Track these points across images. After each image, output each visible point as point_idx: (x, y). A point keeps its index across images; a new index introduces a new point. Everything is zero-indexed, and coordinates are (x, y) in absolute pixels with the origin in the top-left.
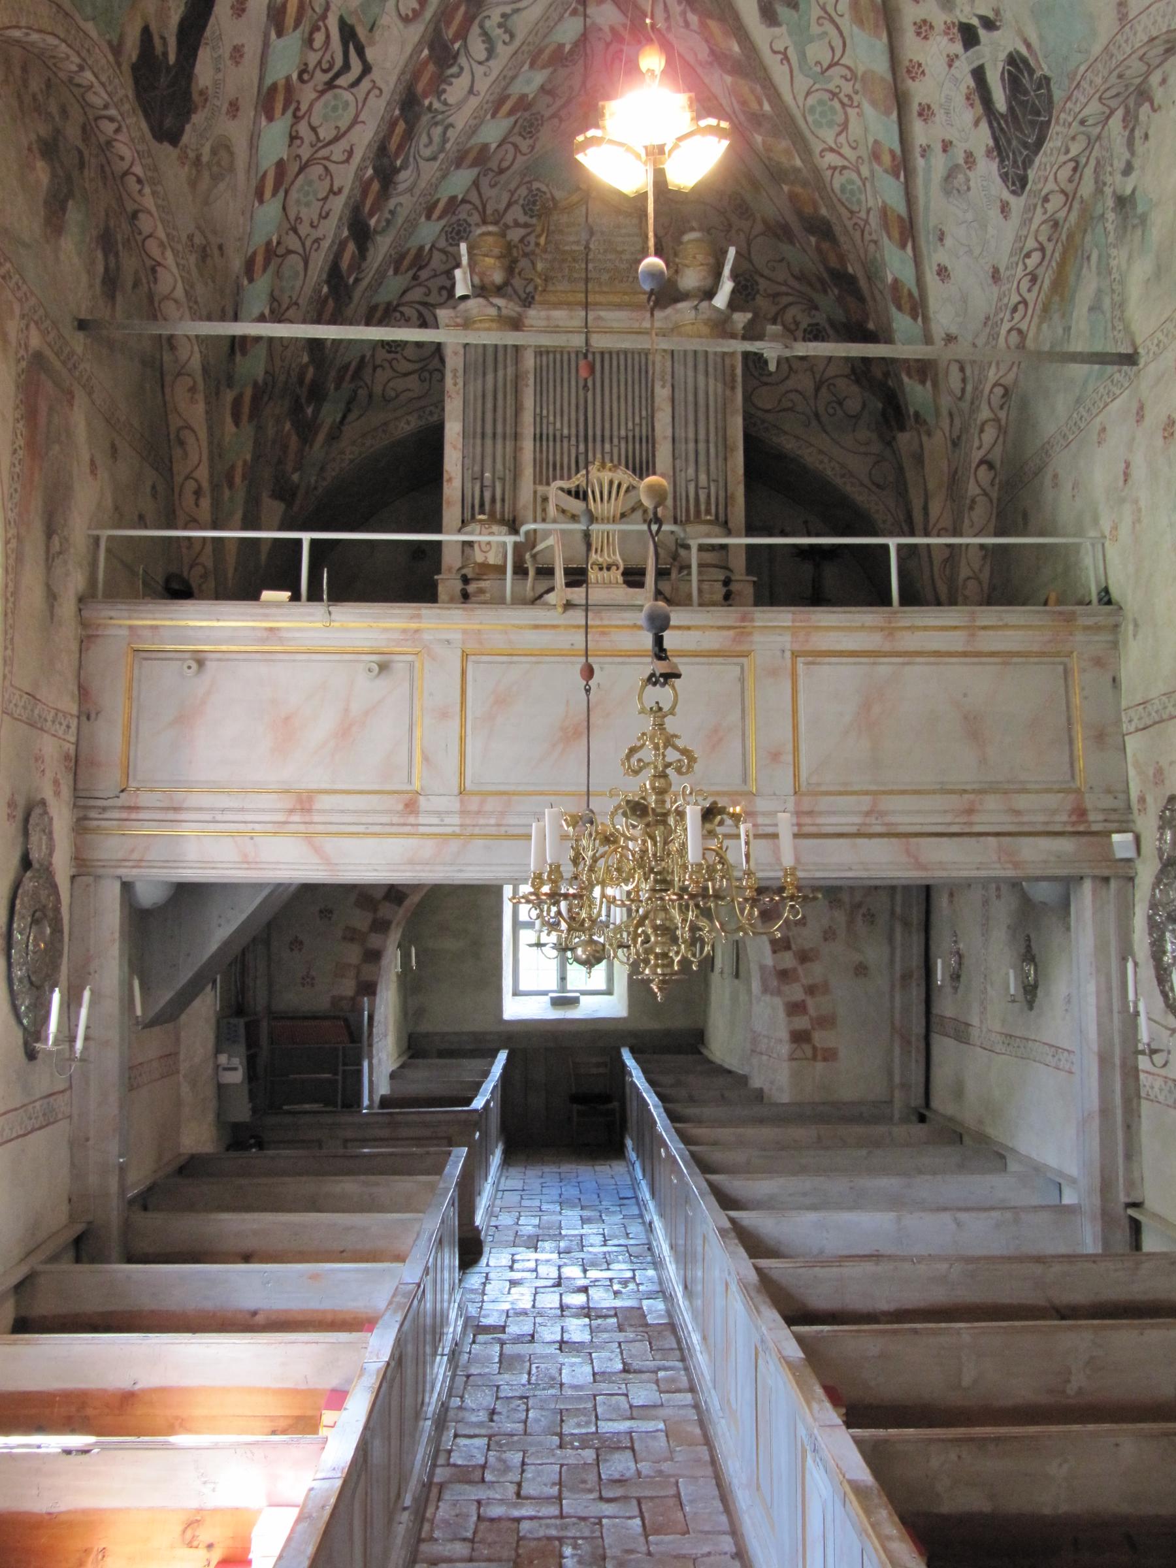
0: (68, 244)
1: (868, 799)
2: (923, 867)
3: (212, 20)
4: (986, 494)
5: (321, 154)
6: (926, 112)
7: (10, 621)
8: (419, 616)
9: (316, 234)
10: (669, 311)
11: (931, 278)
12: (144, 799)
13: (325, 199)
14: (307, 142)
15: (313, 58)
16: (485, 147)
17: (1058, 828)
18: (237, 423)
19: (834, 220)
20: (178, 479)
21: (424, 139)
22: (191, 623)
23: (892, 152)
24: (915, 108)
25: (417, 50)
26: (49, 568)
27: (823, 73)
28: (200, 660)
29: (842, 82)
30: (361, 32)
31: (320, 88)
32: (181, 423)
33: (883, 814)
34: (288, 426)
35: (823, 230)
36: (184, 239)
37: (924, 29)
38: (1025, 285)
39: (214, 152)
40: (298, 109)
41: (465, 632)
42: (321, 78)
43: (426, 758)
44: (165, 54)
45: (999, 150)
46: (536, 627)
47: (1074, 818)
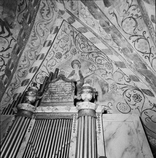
13: (2, 66)
27: (126, 13)
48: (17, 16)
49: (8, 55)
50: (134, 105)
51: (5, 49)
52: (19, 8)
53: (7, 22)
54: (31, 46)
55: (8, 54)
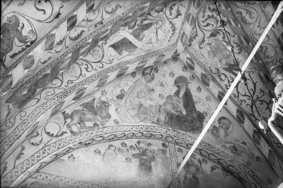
49: (261, 93)
51: (253, 89)
53: (231, 65)
54: (270, 60)
55: (260, 91)
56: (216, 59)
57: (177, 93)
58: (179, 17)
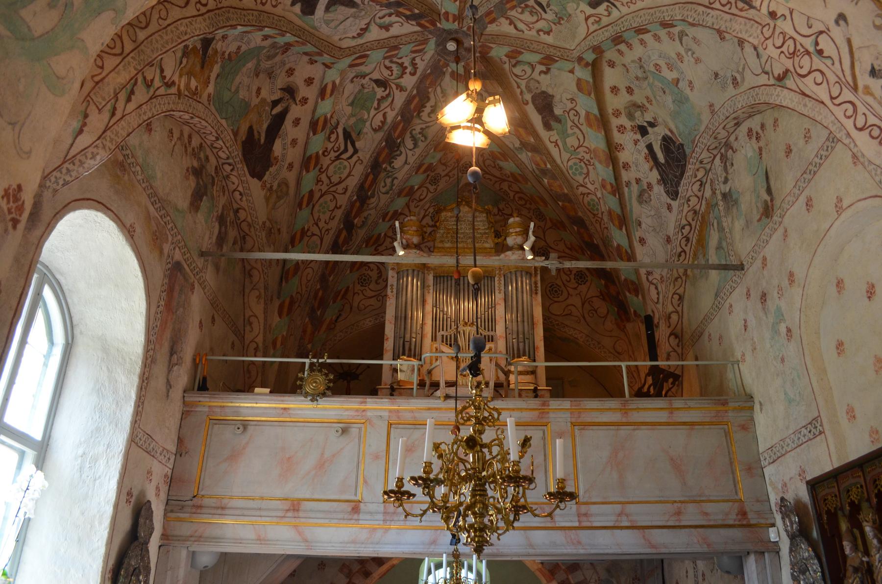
0: (200, 217)
1: (619, 506)
2: (653, 547)
3: (283, 127)
4: (675, 351)
5: (331, 189)
6: (626, 166)
7: (143, 393)
8: (365, 402)
9: (326, 227)
10: (502, 256)
11: (636, 244)
12: (206, 502)
14: (325, 183)
15: (330, 146)
16: (412, 187)
17: (731, 522)
18: (280, 316)
19: (585, 218)
20: (247, 342)
21: (383, 184)
22: (242, 405)
23: (611, 184)
24: (621, 164)
25: (380, 142)
26: (170, 370)
28: (245, 425)
29: (585, 155)
30: (354, 135)
31: (333, 159)
32: (251, 314)
33: (627, 515)
34: (307, 319)
35: (580, 222)
36: (261, 223)
37: (621, 129)
38: (683, 242)
39: (279, 185)
40: (321, 168)
41: (390, 411)
42: (333, 155)
43: (365, 482)
44: (259, 140)
45: (663, 180)
46: (429, 409)
47: (740, 517)
48: (371, 116)
50: (575, 289)
52: (379, 104)
56: (349, 110)
57: (275, 103)
58: (383, 30)
